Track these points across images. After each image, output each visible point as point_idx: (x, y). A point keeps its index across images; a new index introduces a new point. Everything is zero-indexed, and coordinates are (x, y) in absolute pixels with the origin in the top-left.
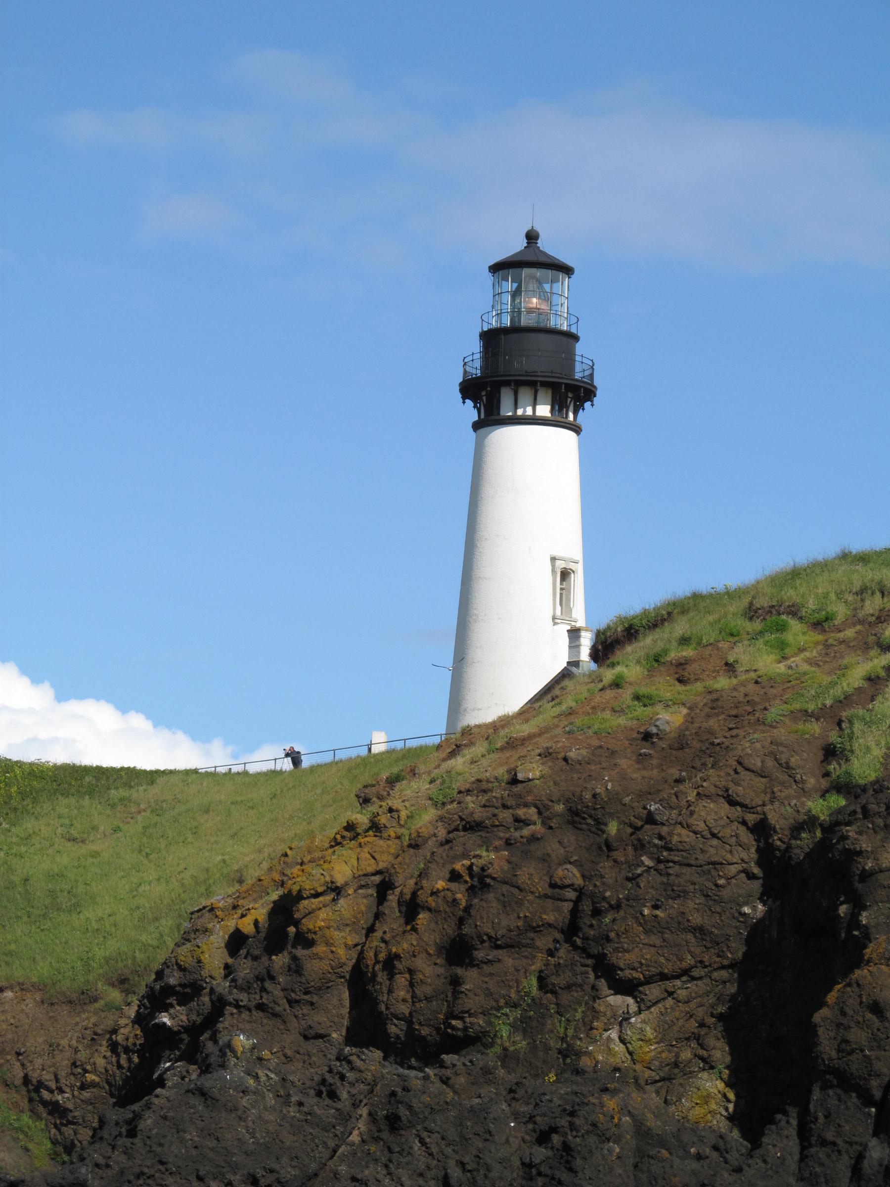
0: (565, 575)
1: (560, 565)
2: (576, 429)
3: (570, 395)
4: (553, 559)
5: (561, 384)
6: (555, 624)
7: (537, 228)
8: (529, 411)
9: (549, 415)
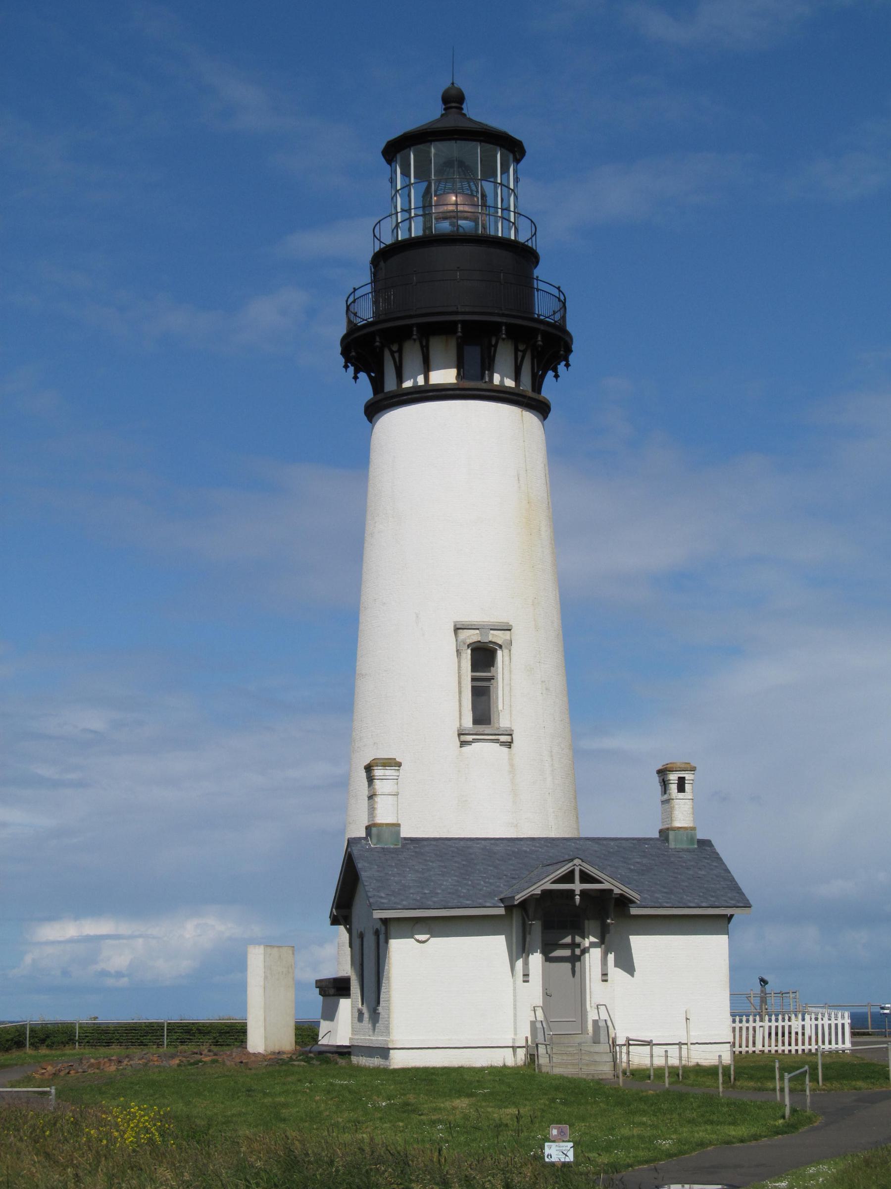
0: (483, 656)
1: (473, 636)
3: (493, 342)
4: (457, 629)
5: (455, 323)
6: (463, 744)
8: (421, 380)
9: (454, 381)
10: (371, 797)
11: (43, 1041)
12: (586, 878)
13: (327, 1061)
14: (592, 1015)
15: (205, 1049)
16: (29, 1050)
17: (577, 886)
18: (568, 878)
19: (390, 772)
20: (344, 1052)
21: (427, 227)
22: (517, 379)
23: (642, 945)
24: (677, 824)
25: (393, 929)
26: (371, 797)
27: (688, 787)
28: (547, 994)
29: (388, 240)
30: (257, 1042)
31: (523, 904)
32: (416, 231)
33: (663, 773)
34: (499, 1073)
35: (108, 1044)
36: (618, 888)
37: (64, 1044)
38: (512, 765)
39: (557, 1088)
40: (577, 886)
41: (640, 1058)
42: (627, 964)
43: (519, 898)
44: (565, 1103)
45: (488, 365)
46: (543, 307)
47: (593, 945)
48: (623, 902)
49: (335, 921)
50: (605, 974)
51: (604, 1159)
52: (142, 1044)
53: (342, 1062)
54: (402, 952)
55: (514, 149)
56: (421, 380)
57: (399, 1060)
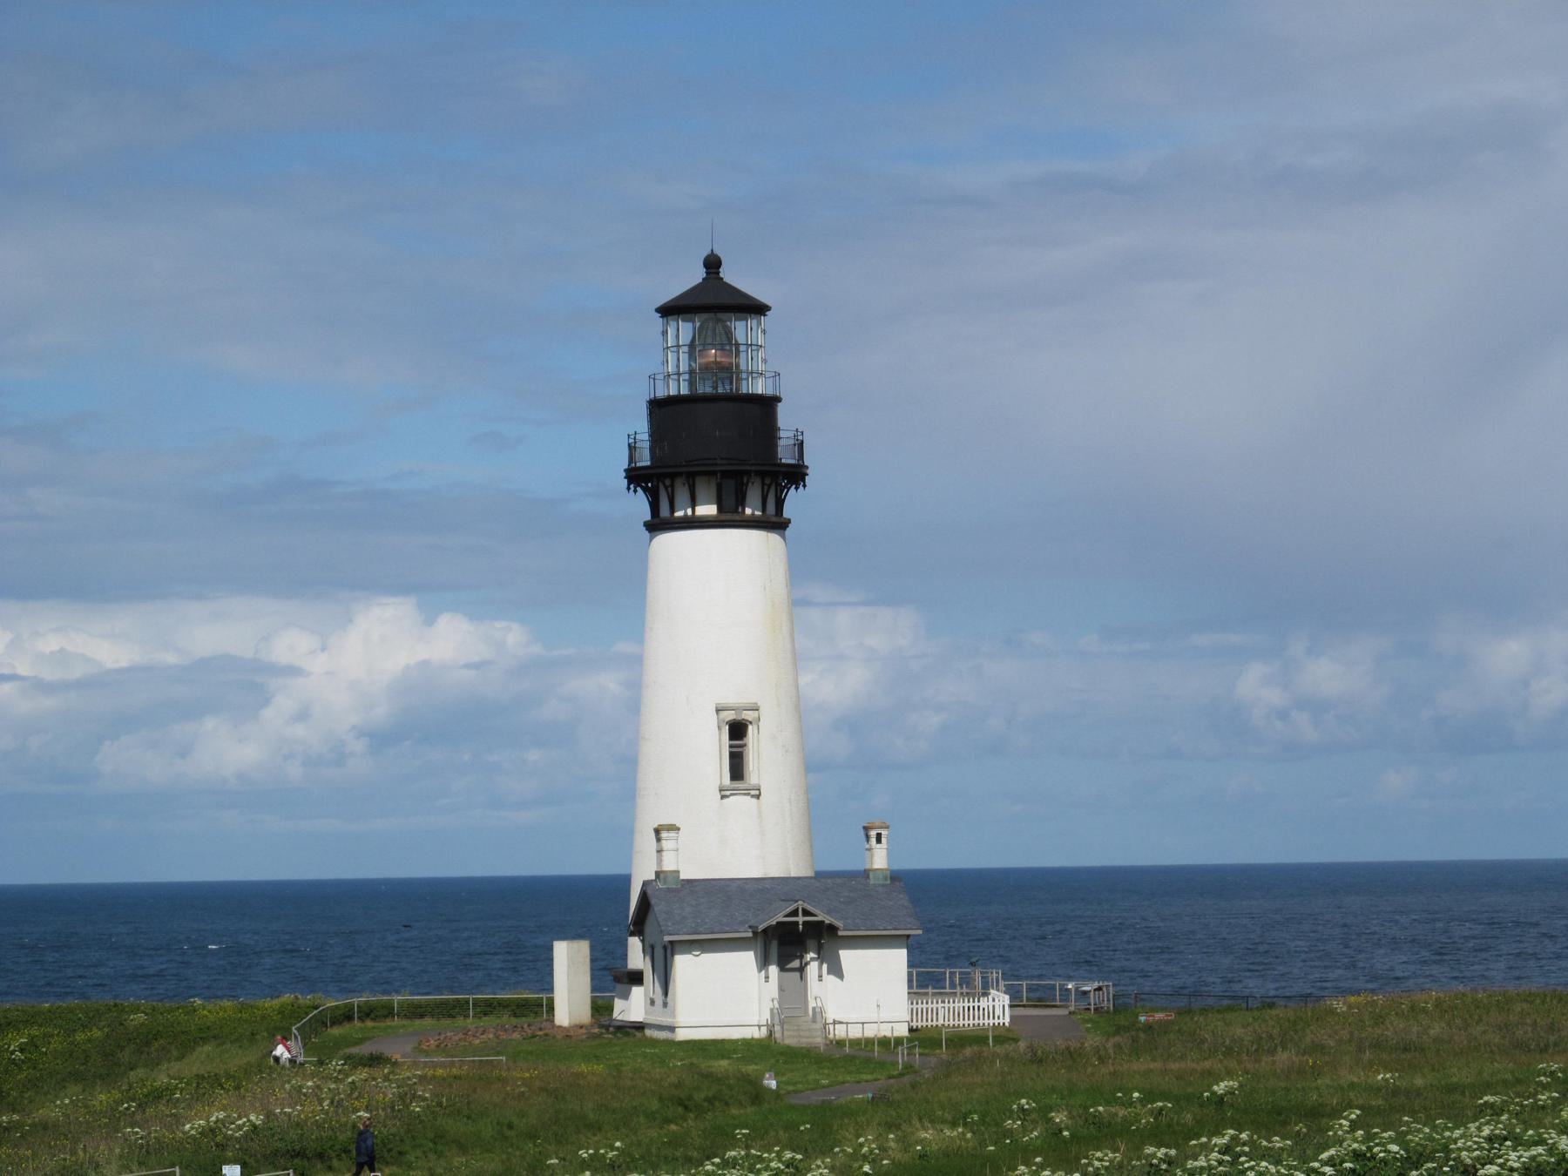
0: (738, 730)
1: (730, 716)
2: (775, 523)
4: (718, 711)
6: (723, 797)
7: (717, 252)
10: (659, 851)
11: (368, 1015)
12: (806, 913)
13: (628, 1034)
14: (812, 1004)
15: (505, 1018)
16: (357, 1023)
17: (801, 919)
18: (795, 913)
19: (672, 834)
20: (640, 1027)
21: (692, 383)
22: (764, 509)
23: (847, 956)
24: (876, 866)
25: (677, 947)
26: (659, 851)
27: (884, 840)
28: (781, 989)
31: (765, 931)
32: (684, 391)
33: (866, 829)
34: (748, 1044)
35: (422, 1016)
36: (828, 920)
37: (386, 1016)
38: (760, 812)
39: (781, 1054)
40: (801, 919)
41: (840, 1032)
42: (837, 970)
43: (761, 927)
44: (785, 1062)
45: (741, 501)
47: (813, 959)
48: (832, 929)
50: (820, 976)
51: (791, 1088)
52: (452, 1016)
53: (638, 1034)
54: (683, 964)
56: (689, 512)
57: (682, 1035)
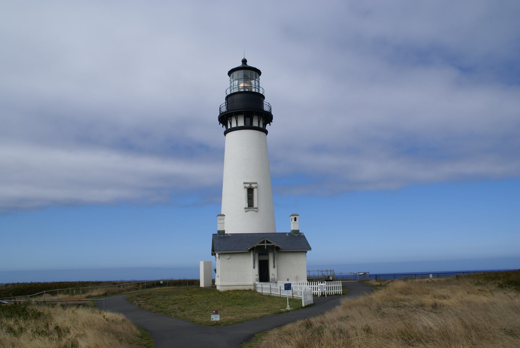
1: (248, 186)
6: (246, 211)
7: (246, 58)
12: (268, 242)
17: (265, 244)
18: (263, 242)
29: (229, 93)
30: (202, 285)
36: (276, 245)
46: (266, 108)
48: (278, 249)
49: (212, 255)
55: (259, 72)
